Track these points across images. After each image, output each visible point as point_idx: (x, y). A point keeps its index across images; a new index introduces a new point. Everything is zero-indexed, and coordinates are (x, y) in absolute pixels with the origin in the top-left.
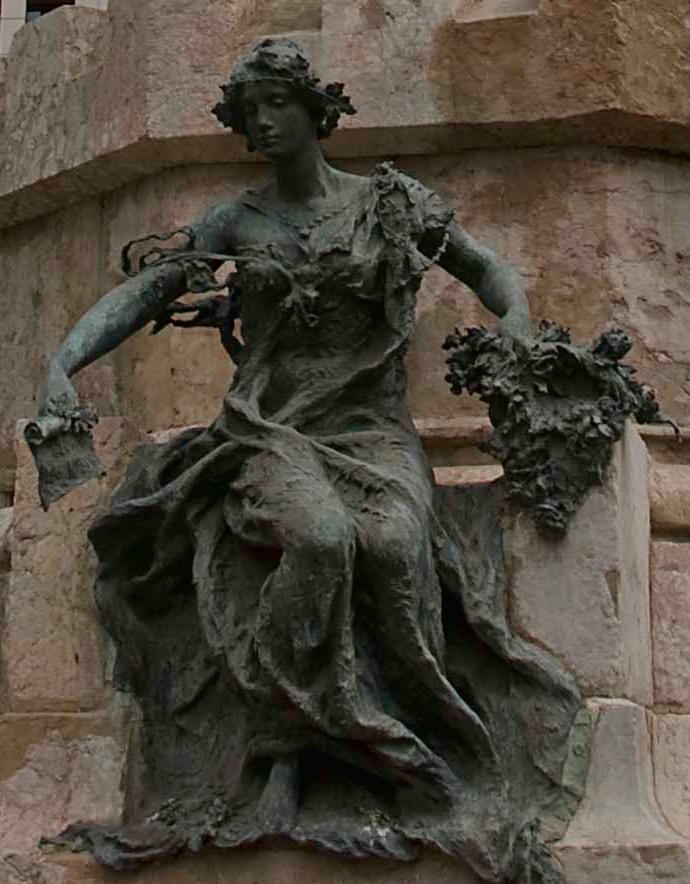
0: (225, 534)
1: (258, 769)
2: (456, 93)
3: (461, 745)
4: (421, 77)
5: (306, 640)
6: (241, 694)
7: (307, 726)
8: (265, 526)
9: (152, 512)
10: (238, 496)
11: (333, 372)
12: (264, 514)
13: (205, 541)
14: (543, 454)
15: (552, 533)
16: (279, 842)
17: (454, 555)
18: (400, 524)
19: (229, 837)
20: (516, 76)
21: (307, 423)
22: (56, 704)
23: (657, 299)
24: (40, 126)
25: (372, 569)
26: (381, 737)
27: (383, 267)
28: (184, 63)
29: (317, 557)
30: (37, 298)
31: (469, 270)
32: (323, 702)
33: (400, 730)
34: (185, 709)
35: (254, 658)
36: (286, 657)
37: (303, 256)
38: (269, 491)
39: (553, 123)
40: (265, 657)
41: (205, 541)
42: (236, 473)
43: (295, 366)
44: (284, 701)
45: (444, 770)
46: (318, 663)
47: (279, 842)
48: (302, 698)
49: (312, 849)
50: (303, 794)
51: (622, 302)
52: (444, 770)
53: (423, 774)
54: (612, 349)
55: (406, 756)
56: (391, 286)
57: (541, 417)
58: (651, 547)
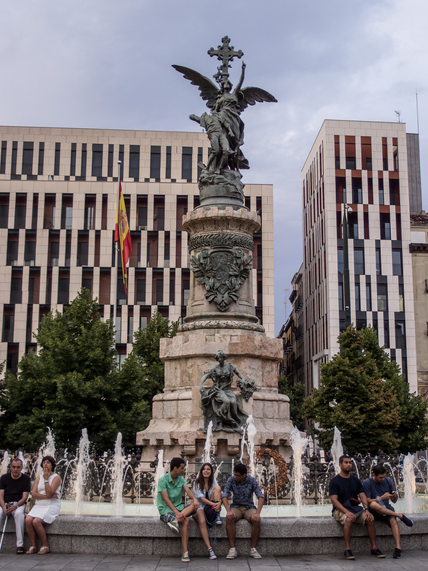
0: (215, 400)
1: (218, 423)
2: (230, 350)
3: (239, 421)
4: (226, 348)
5: (225, 411)
6: (217, 416)
7: (225, 419)
8: (221, 400)
9: (208, 398)
10: (217, 397)
11: (224, 385)
12: (221, 399)
13: (213, 401)
14: (246, 394)
15: (247, 401)
16: (222, 430)
17: (238, 403)
18: (234, 400)
19: (217, 430)
20: (237, 349)
21: (223, 389)
22: (197, 417)
23: (250, 373)
24: (179, 349)
25: (231, 405)
26: (232, 421)
27: (230, 374)
28: (200, 345)
29: (227, 404)
30: (176, 368)
31: (237, 374)
32: (226, 417)
33: (234, 420)
34: (210, 417)
35: (219, 412)
36: (223, 412)
37: (223, 373)
38: (221, 397)
39: (240, 354)
40: (221, 413)
41: (213, 401)
42: (216, 394)
43: (221, 384)
44: (222, 417)
45: (237, 424)
46: (226, 414)
47: (222, 430)
48: (225, 417)
49: (225, 431)
50: (223, 426)
51: (247, 374)
52: (237, 424)
53: (235, 424)
54: (253, 383)
55: (234, 422)
56: (231, 376)
57: (246, 390)
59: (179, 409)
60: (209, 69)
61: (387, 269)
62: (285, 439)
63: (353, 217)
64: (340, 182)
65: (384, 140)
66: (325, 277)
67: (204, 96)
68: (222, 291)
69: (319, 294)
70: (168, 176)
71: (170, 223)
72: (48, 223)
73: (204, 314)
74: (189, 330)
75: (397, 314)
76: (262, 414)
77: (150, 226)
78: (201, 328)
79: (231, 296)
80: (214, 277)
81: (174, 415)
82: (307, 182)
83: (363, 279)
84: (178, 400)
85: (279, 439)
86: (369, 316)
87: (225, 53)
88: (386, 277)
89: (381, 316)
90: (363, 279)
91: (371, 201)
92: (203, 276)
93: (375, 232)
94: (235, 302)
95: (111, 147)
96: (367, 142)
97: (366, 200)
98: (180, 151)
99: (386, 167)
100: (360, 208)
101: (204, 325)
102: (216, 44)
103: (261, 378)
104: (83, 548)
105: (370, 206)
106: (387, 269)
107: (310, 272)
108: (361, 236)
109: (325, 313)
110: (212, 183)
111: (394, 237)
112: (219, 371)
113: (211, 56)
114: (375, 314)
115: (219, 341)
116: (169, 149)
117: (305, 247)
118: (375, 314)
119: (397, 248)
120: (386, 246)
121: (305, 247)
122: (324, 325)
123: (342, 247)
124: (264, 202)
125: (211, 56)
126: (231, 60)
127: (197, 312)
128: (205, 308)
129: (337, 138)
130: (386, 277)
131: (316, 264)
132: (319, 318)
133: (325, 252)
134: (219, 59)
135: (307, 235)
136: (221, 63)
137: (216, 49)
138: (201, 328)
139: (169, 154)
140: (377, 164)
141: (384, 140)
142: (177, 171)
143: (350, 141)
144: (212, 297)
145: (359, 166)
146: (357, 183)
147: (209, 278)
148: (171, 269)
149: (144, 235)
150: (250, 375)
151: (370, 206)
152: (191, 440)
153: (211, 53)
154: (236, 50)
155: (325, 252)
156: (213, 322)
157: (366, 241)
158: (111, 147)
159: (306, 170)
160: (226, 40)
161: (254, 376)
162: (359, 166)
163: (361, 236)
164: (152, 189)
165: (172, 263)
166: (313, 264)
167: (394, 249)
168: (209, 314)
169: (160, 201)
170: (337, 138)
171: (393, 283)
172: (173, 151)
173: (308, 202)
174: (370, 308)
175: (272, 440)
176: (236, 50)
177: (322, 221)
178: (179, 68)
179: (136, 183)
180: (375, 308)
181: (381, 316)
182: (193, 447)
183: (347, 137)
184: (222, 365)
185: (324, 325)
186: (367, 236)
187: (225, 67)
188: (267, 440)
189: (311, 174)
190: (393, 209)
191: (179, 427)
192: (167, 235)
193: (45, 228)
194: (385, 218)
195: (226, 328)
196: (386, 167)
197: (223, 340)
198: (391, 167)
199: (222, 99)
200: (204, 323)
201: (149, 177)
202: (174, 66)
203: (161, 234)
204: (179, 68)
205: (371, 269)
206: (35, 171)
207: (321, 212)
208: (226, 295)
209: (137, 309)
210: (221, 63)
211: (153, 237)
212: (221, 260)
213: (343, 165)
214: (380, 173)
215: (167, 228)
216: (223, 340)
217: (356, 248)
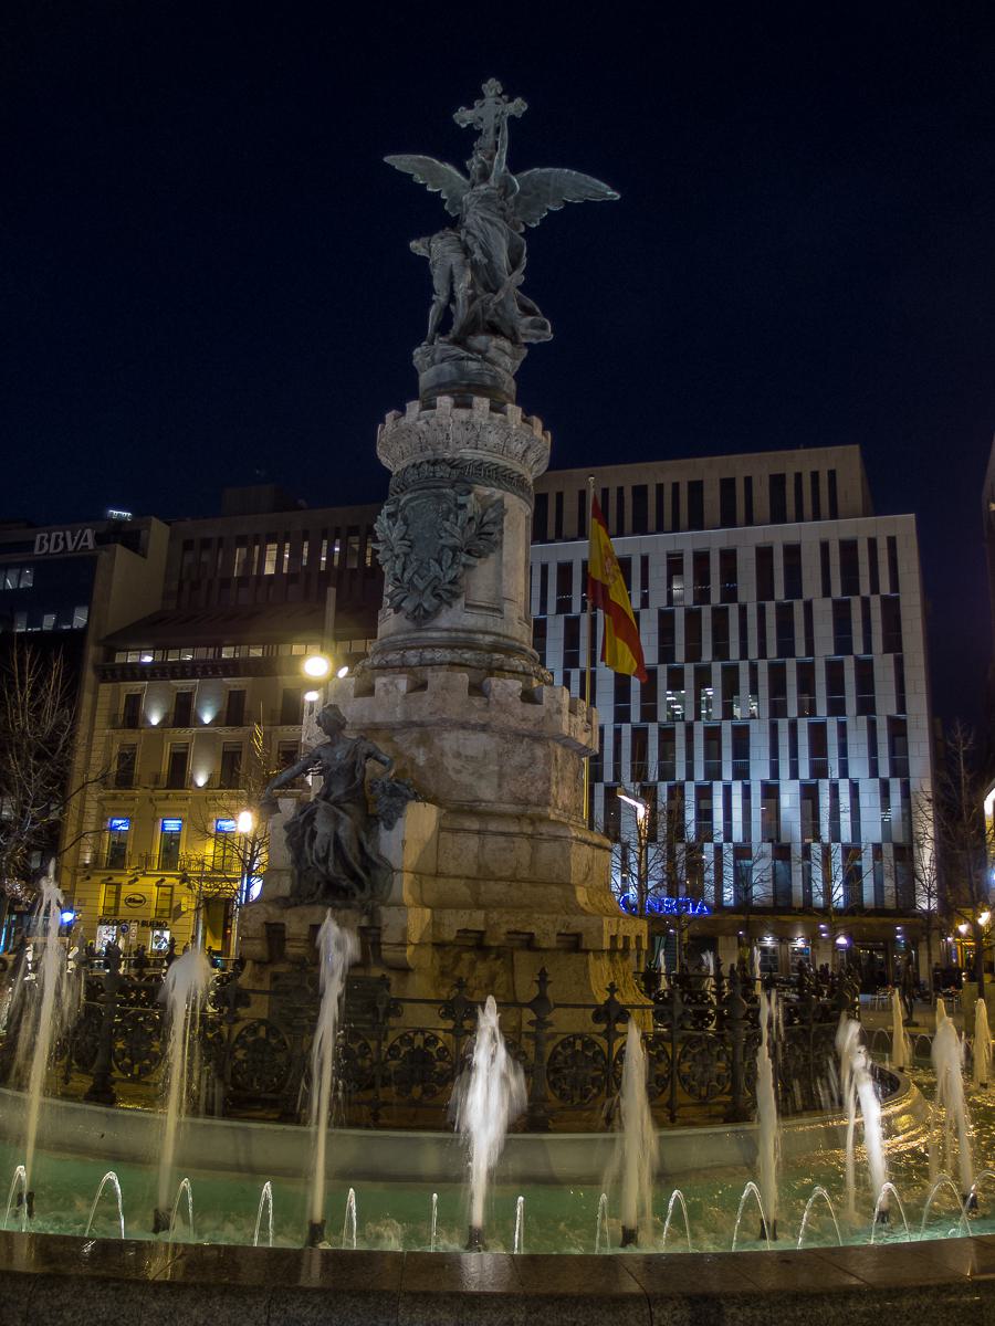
5: (322, 855)
20: (420, 709)
36: (319, 861)
48: (323, 869)
55: (344, 884)
58: (439, 836)
62: (527, 931)
71: (747, 590)
72: (564, 606)
76: (475, 867)
79: (441, 592)
85: (504, 929)
95: (660, 487)
103: (496, 780)
115: (382, 693)
116: (748, 481)
150: (459, 772)
158: (660, 487)
161: (473, 774)
165: (753, 653)
175: (482, 933)
182: (256, 942)
188: (459, 931)
192: (743, 610)
193: (559, 611)
197: (391, 688)
203: (733, 610)
206: (551, 532)
209: (699, 729)
211: (720, 616)
215: (742, 598)
216: (391, 688)
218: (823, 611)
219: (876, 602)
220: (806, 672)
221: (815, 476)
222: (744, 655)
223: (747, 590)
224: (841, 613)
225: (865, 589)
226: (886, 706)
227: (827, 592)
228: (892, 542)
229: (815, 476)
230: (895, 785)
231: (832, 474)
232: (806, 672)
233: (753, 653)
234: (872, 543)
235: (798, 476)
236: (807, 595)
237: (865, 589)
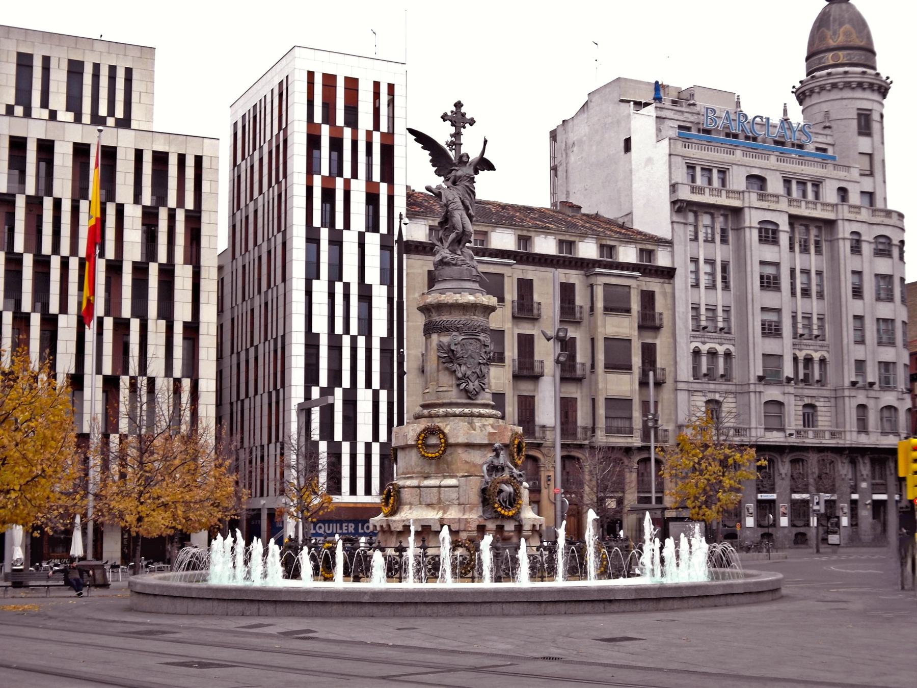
59: (442, 496)
60: (442, 134)
61: (373, 276)
63: (328, 195)
64: (313, 142)
65: (377, 85)
66: (284, 279)
67: (434, 162)
68: (473, 379)
69: (266, 304)
70: (45, 104)
71: (63, 186)
73: (454, 401)
74: (438, 416)
75: (382, 340)
77: (31, 189)
78: (455, 415)
80: (465, 364)
81: (434, 501)
82: (244, 127)
83: (339, 286)
84: (440, 487)
86: (346, 341)
87: (458, 119)
88: (370, 286)
89: (361, 341)
90: (339, 286)
91: (355, 175)
92: (452, 362)
93: (359, 220)
94: (484, 390)
96: (352, 85)
97: (347, 173)
98: (65, 66)
99: (377, 126)
100: (339, 183)
101: (457, 412)
102: (450, 109)
104: (512, 611)
105: (353, 181)
106: (373, 276)
107: (244, 267)
108: (339, 225)
109: (281, 333)
110: (455, 265)
111: (384, 229)
112: (496, 462)
113: (444, 120)
114: (354, 340)
116: (46, 60)
117: (234, 226)
118: (354, 340)
119: (386, 246)
120: (373, 241)
121: (234, 226)
122: (276, 351)
123: (312, 238)
124: (205, 163)
125: (444, 120)
126: (464, 128)
127: (444, 398)
128: (453, 395)
129: (311, 75)
130: (370, 286)
131: (260, 258)
132: (266, 339)
133: (284, 244)
134: (452, 125)
135: (239, 208)
136: (453, 130)
137: (449, 114)
138: (455, 415)
139: (46, 69)
140: (365, 120)
141: (377, 85)
142: (58, 100)
143: (329, 80)
144: (464, 385)
145: (340, 120)
146: (336, 144)
147: (460, 365)
148: (62, 257)
149: (20, 202)
151: (353, 181)
152: (474, 526)
153: (444, 117)
154: (468, 116)
155: (284, 244)
156: (467, 411)
157: (345, 232)
159: (245, 107)
160: (458, 105)
162: (340, 120)
163: (339, 224)
164: (34, 131)
165: (65, 250)
166: (253, 254)
167: (383, 247)
168: (459, 401)
169: (46, 148)
170: (311, 75)
171: (380, 295)
172: (53, 64)
173: (243, 158)
174: (347, 330)
176: (468, 116)
177: (280, 196)
178: (411, 131)
179: (7, 118)
180: (354, 330)
181: (361, 341)
183: (324, 75)
184: (497, 456)
185: (276, 351)
186: (347, 226)
187: (457, 135)
189: (255, 117)
190: (384, 187)
191: (444, 513)
192: (57, 203)
194: (372, 199)
195: (478, 416)
196: (377, 126)
198: (384, 127)
199: (459, 173)
200: (457, 410)
201: (12, 102)
202: (408, 129)
203: (48, 203)
204: (411, 131)
205: (350, 273)
207: (278, 182)
208: (476, 383)
210: (453, 130)
211: (34, 205)
212: (471, 347)
213: (318, 118)
214: (369, 134)
215: (57, 193)
217: (331, 242)
218: (133, 214)
219: (180, 216)
220: (114, 268)
221: (113, 69)
222: (56, 248)
223: (63, 186)
224: (149, 218)
225: (172, 202)
226: (182, 312)
227: (137, 199)
228: (199, 160)
229: (113, 69)
230: (186, 383)
231: (129, 72)
232: (114, 268)
233: (65, 250)
234: (182, 158)
235: (96, 67)
236: (119, 200)
237: (172, 202)
